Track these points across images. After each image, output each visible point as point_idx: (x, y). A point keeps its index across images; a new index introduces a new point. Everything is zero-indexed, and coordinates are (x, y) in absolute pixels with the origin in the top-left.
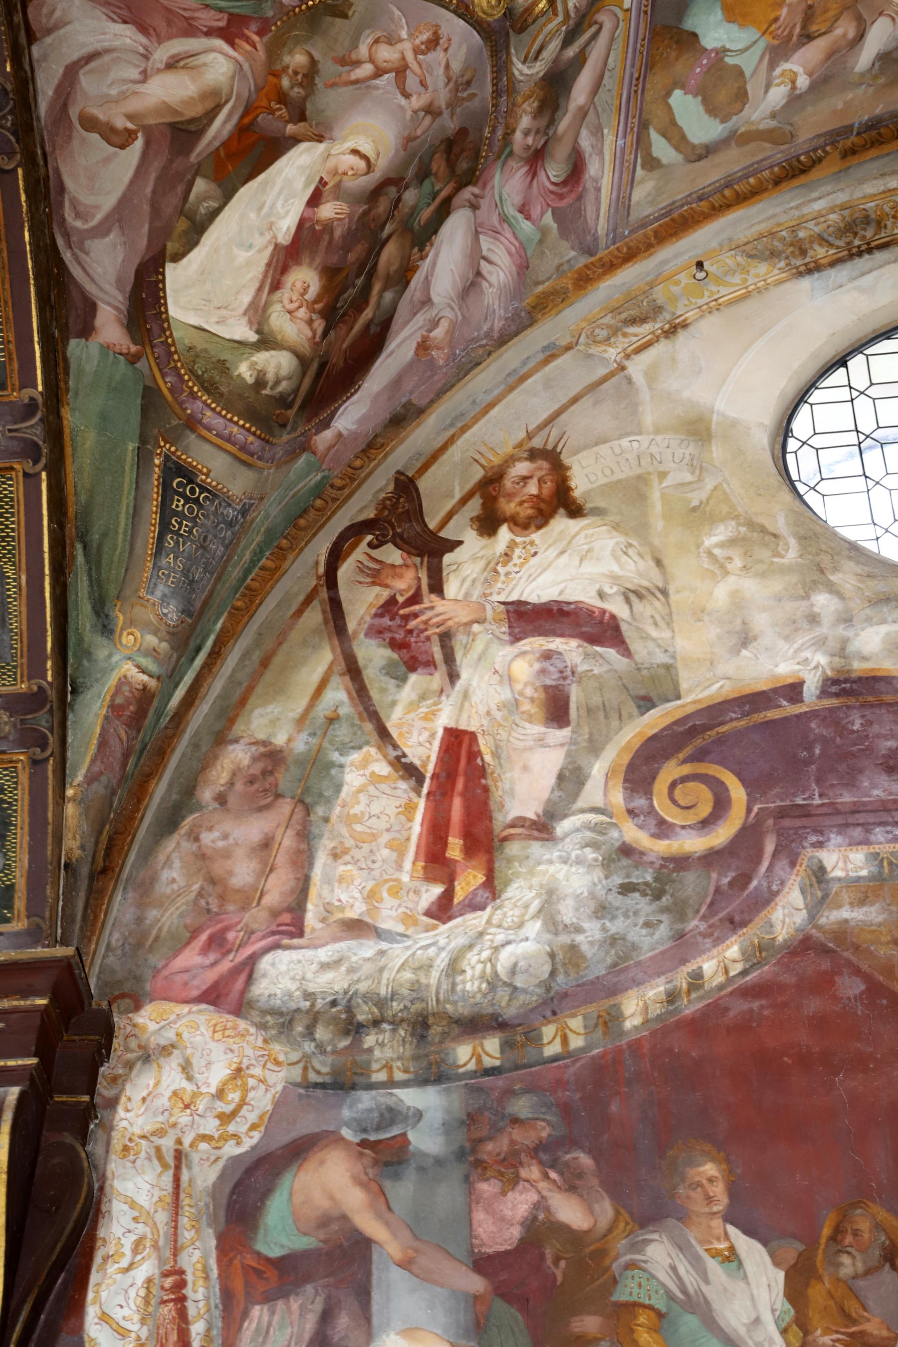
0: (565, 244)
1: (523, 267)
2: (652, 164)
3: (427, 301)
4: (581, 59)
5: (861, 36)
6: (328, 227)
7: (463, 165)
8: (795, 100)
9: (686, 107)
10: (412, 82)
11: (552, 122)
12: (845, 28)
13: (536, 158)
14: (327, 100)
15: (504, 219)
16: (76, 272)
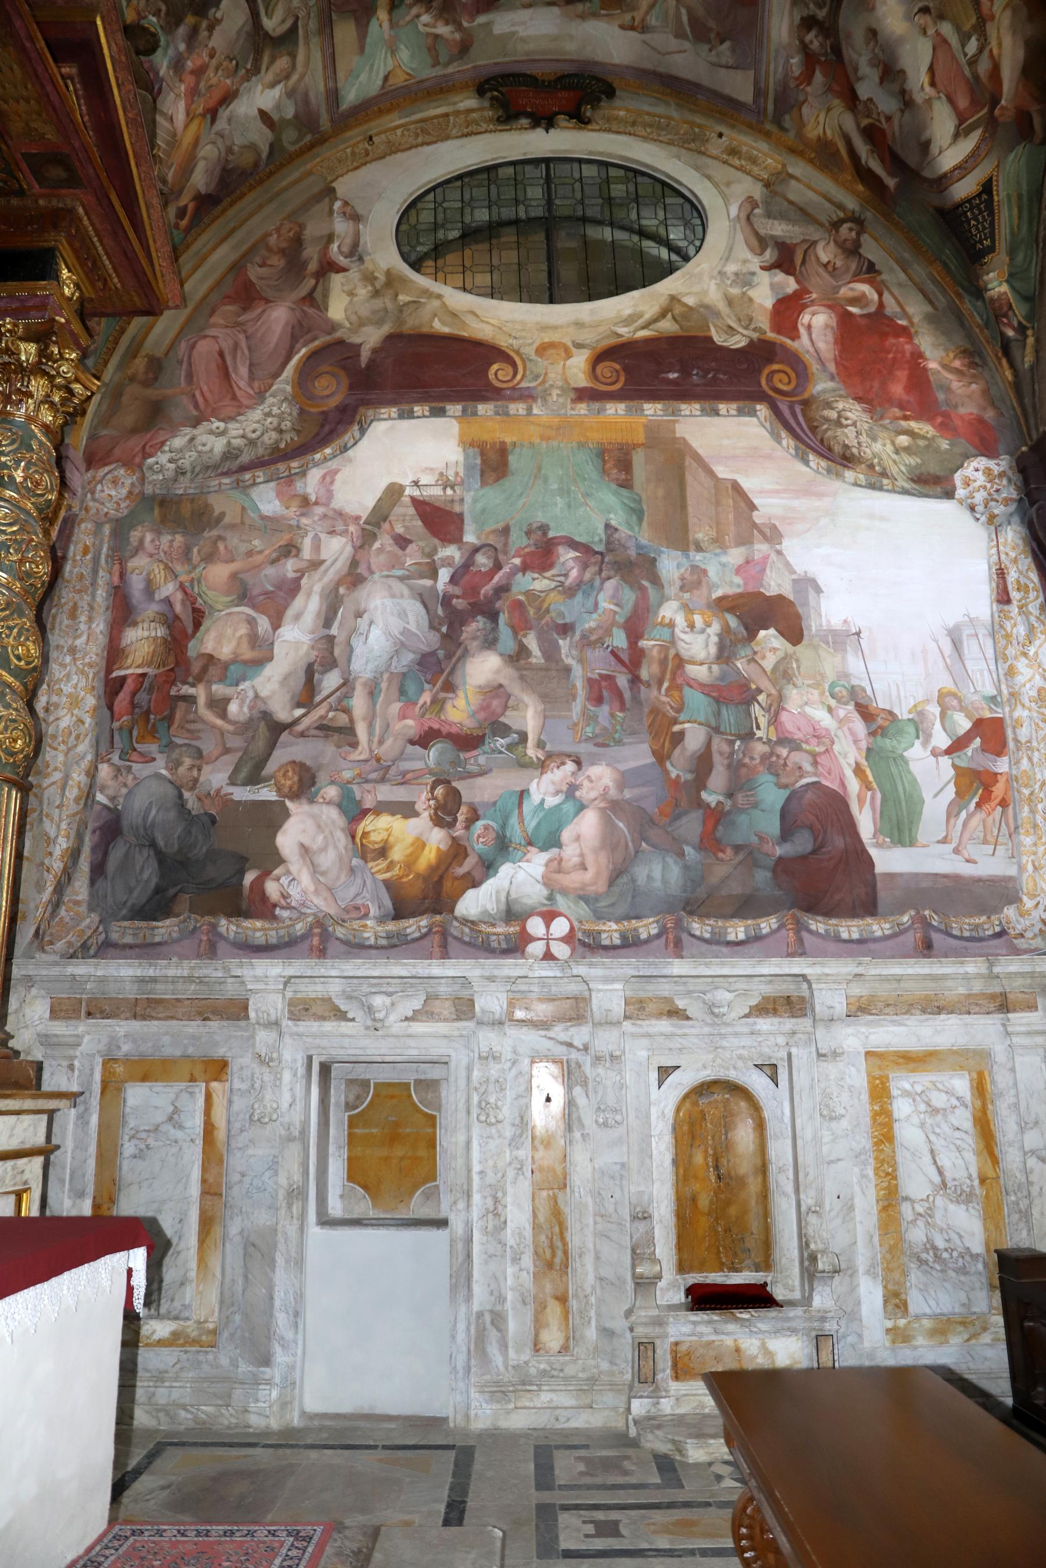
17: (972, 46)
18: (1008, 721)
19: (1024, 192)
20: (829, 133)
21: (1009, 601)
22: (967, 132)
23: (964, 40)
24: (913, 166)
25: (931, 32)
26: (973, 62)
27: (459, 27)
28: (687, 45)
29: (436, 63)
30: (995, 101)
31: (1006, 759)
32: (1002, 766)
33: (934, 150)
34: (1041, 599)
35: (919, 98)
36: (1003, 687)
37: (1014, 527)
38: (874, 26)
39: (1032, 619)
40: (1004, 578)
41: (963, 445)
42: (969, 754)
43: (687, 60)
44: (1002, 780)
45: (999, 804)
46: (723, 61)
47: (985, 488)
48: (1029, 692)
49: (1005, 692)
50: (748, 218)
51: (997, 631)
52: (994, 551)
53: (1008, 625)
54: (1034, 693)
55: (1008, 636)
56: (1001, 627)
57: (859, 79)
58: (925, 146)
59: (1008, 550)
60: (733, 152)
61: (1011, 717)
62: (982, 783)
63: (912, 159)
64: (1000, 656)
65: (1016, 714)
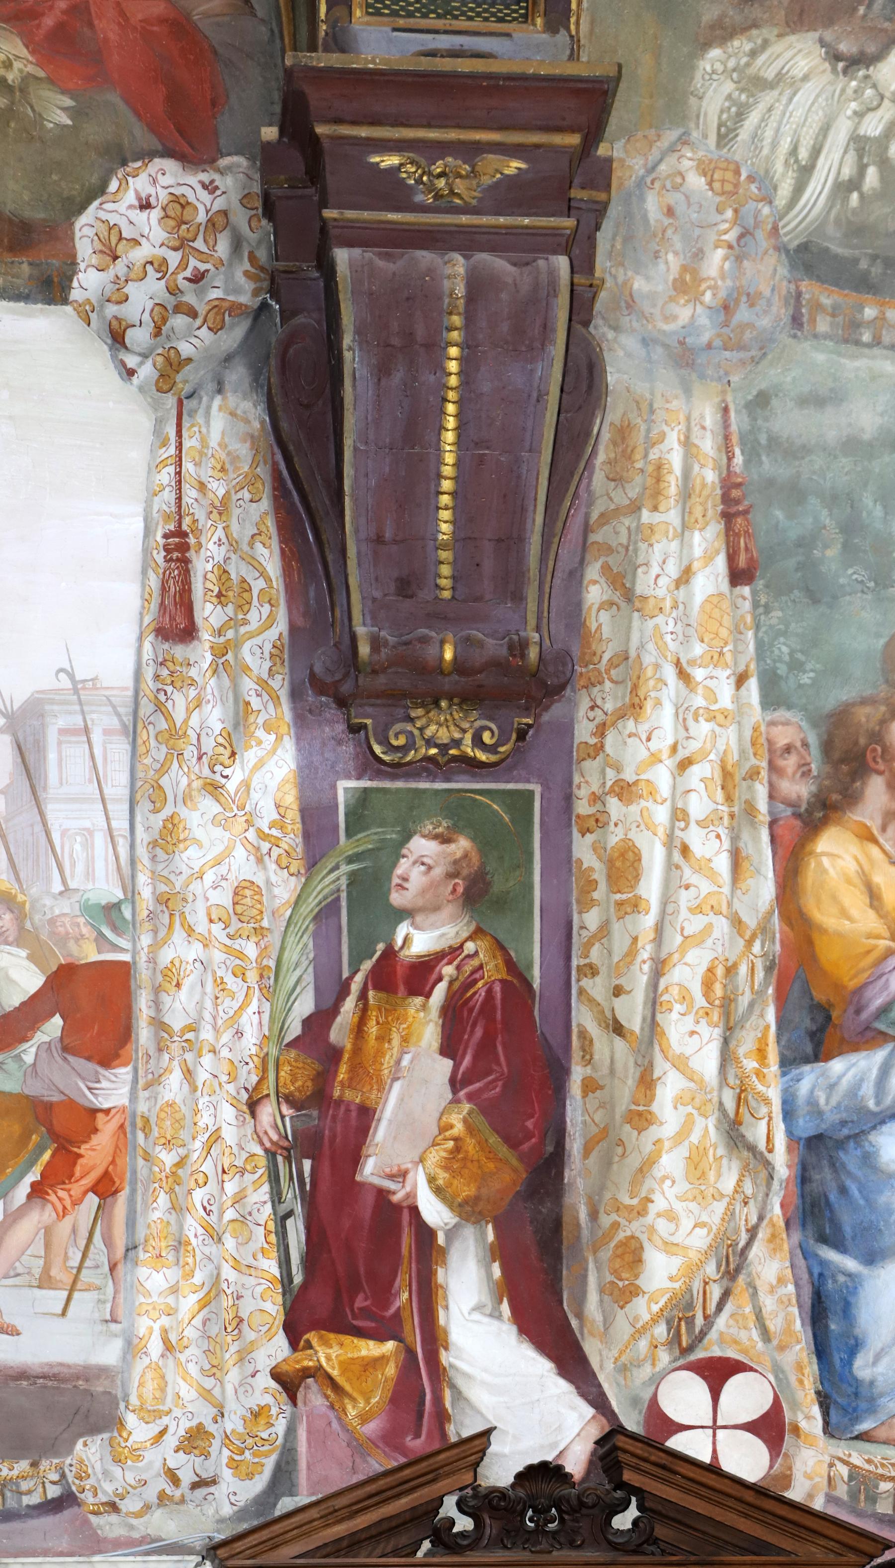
18: (143, 973)
21: (187, 632)
31: (124, 1073)
32: (113, 1090)
34: (281, 626)
36: (143, 878)
37: (232, 399)
39: (248, 685)
40: (185, 562)
41: (116, 116)
42: (29, 1058)
44: (107, 1129)
45: (94, 1189)
47: (161, 266)
48: (210, 895)
49: (146, 892)
51: (146, 718)
52: (166, 475)
53: (178, 704)
54: (223, 898)
55: (173, 736)
56: (159, 707)
59: (206, 473)
61: (152, 960)
62: (54, 1135)
64: (145, 791)
65: (166, 956)
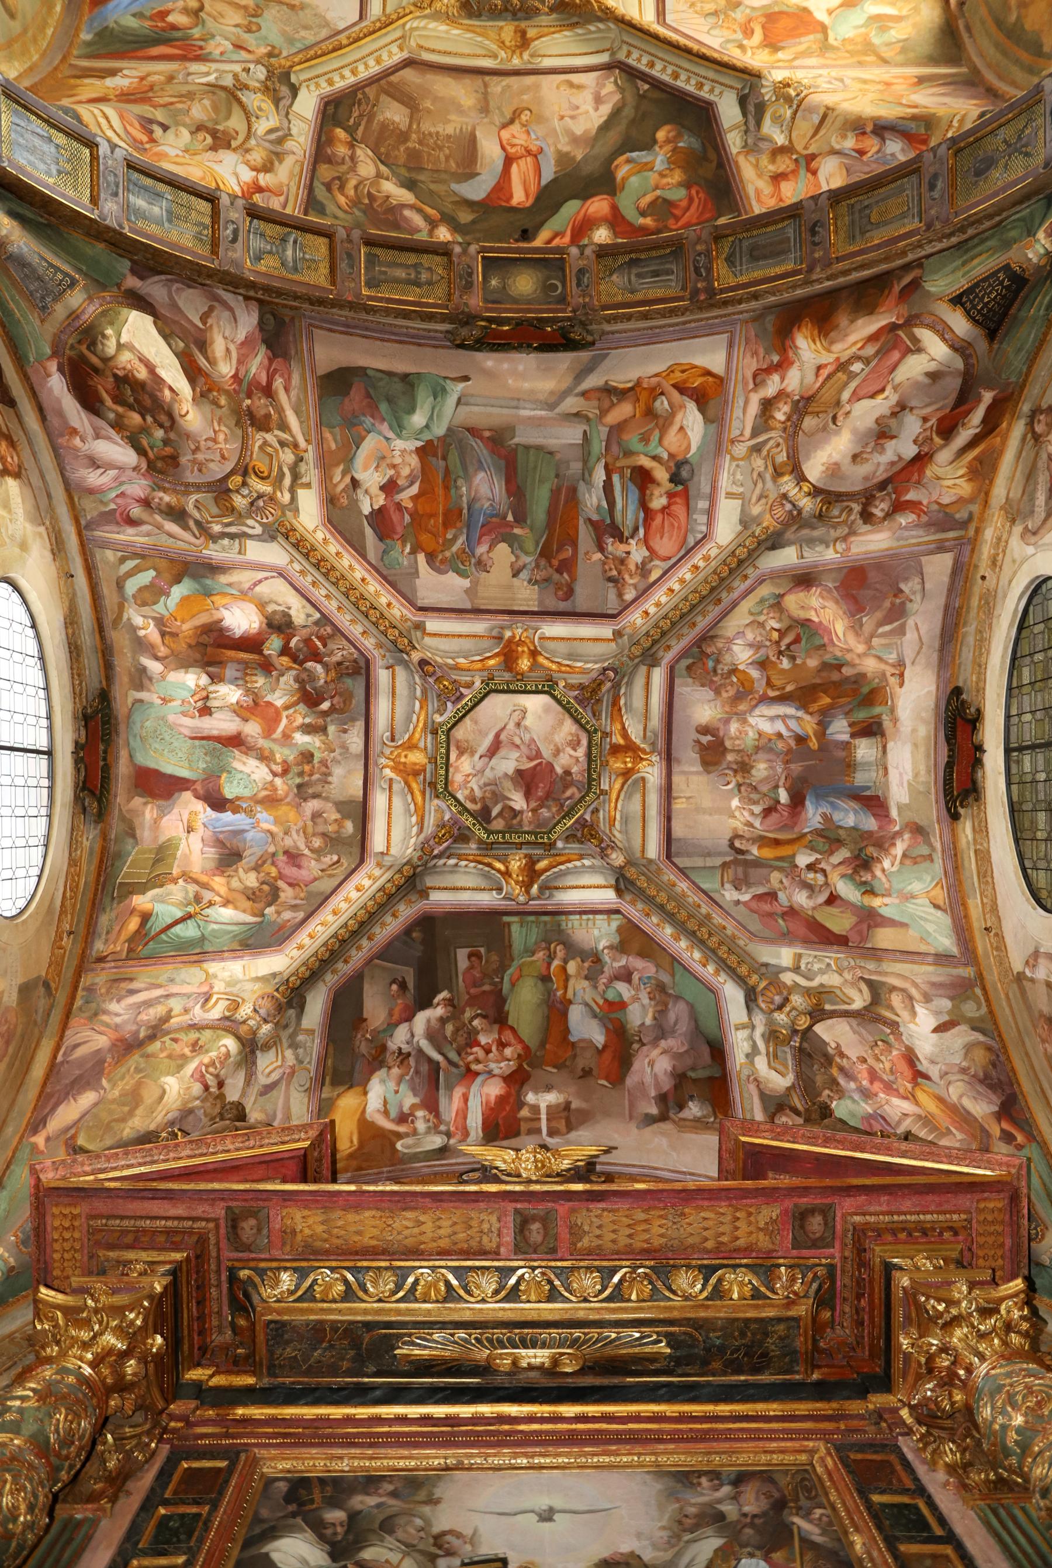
0: (95, 513)
1: (91, 491)
2: (122, 560)
3: (97, 436)
4: (186, 528)
5: (157, 658)
6: (161, 391)
7: (159, 464)
8: (134, 629)
9: (146, 577)
10: (210, 444)
11: (161, 512)
12: (163, 651)
13: (146, 503)
14: (207, 408)
15: (122, 484)
16: (156, 278)
17: (857, 367)
19: (959, 262)
20: (961, 472)
22: (916, 340)
23: (852, 376)
24: (958, 381)
25: (847, 408)
26: (867, 361)
27: (899, 834)
28: (911, 622)
29: (930, 858)
30: (893, 327)
33: (932, 367)
35: (894, 398)
38: (849, 459)
43: (924, 620)
46: (919, 587)
50: (1034, 534)
57: (900, 458)
58: (934, 376)
60: (994, 563)
63: (954, 384)
